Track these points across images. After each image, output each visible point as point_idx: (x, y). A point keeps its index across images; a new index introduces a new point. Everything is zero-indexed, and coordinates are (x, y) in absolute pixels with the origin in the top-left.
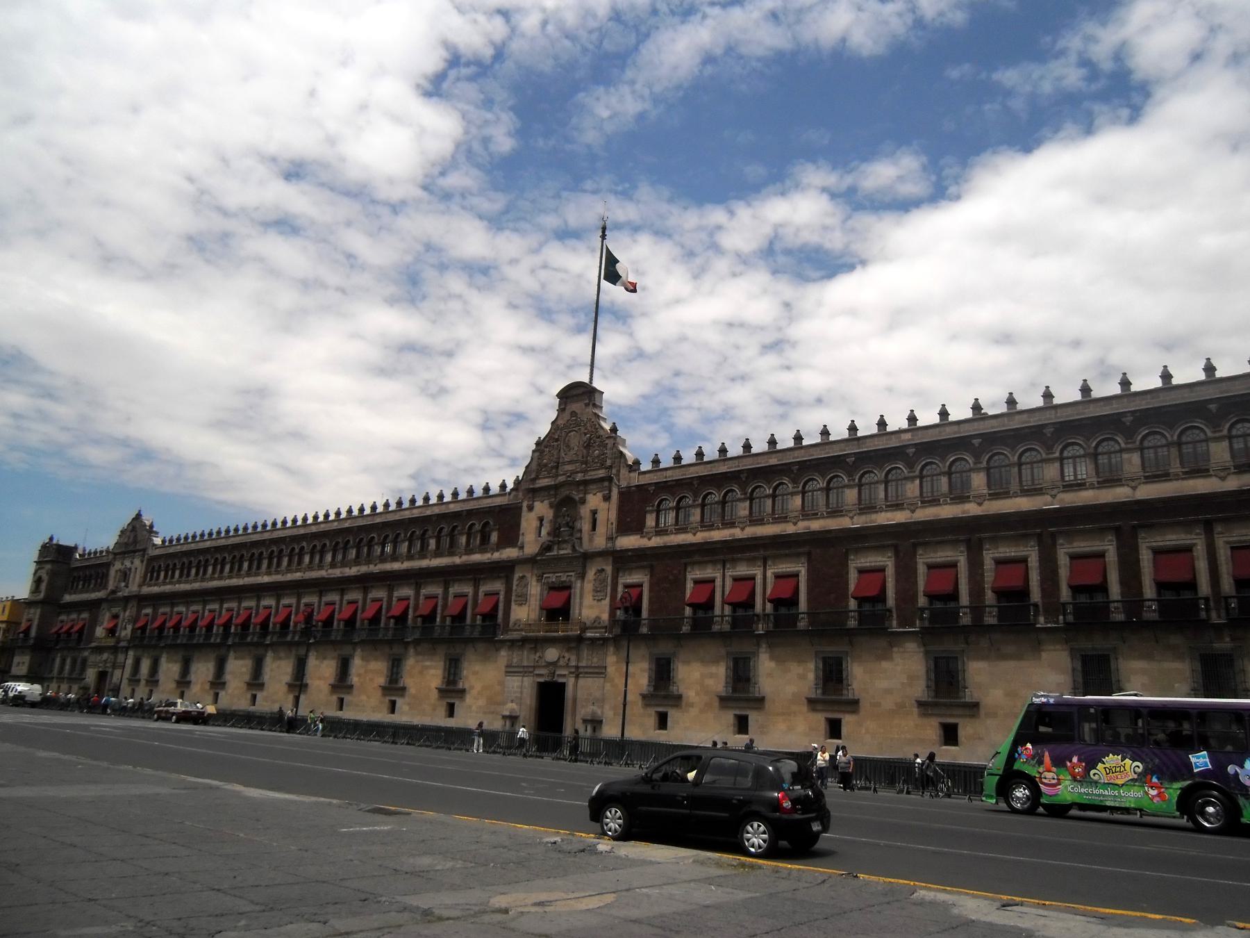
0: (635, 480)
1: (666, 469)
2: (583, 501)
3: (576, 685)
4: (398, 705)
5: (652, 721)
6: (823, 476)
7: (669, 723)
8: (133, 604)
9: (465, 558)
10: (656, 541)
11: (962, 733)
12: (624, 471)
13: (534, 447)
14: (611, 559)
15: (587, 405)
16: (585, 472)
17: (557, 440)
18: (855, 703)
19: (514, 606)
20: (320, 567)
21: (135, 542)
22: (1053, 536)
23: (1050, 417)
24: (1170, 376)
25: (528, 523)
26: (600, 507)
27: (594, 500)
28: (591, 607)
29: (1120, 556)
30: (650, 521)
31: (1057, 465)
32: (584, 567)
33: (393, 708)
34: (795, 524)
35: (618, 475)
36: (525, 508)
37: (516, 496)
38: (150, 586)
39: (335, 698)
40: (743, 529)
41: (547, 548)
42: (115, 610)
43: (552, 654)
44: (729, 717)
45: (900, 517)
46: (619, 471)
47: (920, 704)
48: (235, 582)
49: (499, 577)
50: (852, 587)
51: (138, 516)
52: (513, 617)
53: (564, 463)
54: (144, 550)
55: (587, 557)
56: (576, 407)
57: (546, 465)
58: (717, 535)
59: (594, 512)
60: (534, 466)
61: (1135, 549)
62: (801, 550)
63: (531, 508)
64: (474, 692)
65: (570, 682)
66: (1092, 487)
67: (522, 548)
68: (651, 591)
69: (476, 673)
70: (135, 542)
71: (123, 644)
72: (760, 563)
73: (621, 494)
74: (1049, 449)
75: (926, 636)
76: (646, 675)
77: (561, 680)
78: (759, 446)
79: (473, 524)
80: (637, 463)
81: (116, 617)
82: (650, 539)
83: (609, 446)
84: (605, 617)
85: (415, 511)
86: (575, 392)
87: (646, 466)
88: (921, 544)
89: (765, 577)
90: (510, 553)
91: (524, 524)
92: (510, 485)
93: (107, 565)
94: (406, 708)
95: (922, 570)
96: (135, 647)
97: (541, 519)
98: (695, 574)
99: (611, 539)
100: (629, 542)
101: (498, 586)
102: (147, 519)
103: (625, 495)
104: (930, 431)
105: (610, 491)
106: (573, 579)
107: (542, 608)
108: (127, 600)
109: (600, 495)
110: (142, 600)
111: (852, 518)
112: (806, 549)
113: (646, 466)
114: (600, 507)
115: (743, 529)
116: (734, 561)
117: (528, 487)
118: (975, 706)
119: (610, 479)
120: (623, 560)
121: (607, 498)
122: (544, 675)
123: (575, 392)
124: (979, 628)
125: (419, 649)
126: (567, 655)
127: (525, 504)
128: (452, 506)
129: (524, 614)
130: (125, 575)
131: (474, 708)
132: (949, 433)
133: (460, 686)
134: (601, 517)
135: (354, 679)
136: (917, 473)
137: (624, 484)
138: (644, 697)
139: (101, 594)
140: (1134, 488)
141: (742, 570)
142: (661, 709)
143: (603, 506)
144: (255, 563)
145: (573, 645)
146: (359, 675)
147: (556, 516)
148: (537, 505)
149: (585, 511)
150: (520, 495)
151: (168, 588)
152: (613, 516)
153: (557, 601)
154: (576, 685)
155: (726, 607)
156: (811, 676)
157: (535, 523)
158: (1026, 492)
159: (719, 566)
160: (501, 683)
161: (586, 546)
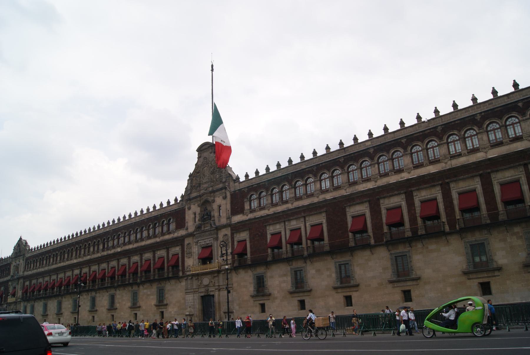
0: (238, 187)
1: (251, 179)
2: (214, 201)
3: (219, 295)
4: (138, 315)
5: (258, 309)
6: (329, 170)
7: (266, 309)
8: (21, 281)
9: (162, 238)
10: (251, 216)
11: (413, 294)
12: (232, 183)
13: (188, 178)
14: (230, 228)
15: (211, 153)
17: (199, 172)
18: (357, 286)
19: (186, 259)
20: (98, 252)
21: (20, 251)
22: (448, 184)
23: (440, 122)
24: (496, 92)
25: (189, 216)
26: (221, 205)
27: (219, 200)
29: (484, 189)
30: (247, 207)
31: (446, 146)
32: (217, 234)
34: (318, 197)
35: (229, 186)
36: (187, 209)
37: (182, 204)
38: (27, 271)
39: (109, 315)
40: (292, 204)
41: (198, 228)
42: (14, 285)
43: (206, 281)
44: (295, 302)
45: (370, 185)
46: (229, 184)
48: (62, 264)
49: (178, 246)
50: (349, 225)
51: (21, 239)
52: (186, 265)
53: (203, 184)
54: (24, 255)
56: (206, 154)
57: (194, 186)
59: (220, 206)
60: (189, 188)
61: (491, 184)
62: (322, 210)
63: (189, 209)
66: (465, 155)
67: (187, 229)
68: (250, 242)
70: (20, 251)
71: (19, 300)
72: (302, 220)
73: (232, 195)
74: (441, 139)
76: (252, 285)
77: (212, 293)
79: (164, 221)
80: (238, 178)
81: (15, 288)
82: (247, 216)
83: (223, 172)
85: (137, 218)
86: (204, 148)
87: (242, 179)
88: (381, 198)
89: (305, 226)
90: (182, 233)
91: (187, 217)
92: (179, 199)
93: (9, 264)
95: (384, 212)
96: (24, 301)
98: (271, 229)
99: (229, 218)
100: (237, 218)
102: (23, 238)
103: (234, 196)
104: (380, 138)
105: (226, 193)
106: (212, 241)
107: (199, 258)
108: (18, 279)
109: (221, 197)
110: (25, 278)
111: (346, 190)
112: (325, 209)
113: (242, 179)
114: (221, 205)
115: (292, 204)
116: (289, 220)
117: (187, 198)
118: (418, 279)
119: (226, 188)
120: (236, 228)
121: (225, 198)
123: (204, 148)
124: (416, 237)
125: (145, 286)
126: (213, 280)
127: (186, 207)
128: (153, 213)
130: (17, 267)
132: (389, 139)
133: (165, 302)
134: (223, 208)
135: (117, 305)
136: (376, 161)
137: (232, 190)
138: (253, 297)
139: (9, 278)
140: (486, 152)
142: (261, 302)
143: (224, 202)
144: (70, 254)
145: (216, 275)
146: (119, 303)
147: (201, 211)
149: (215, 206)
150: (184, 203)
151: (35, 271)
152: (229, 207)
153: (206, 255)
154: (219, 295)
155: (288, 245)
156: (334, 275)
157: (192, 216)
158: (432, 163)
159: (283, 224)
160: (184, 299)
161: (217, 224)
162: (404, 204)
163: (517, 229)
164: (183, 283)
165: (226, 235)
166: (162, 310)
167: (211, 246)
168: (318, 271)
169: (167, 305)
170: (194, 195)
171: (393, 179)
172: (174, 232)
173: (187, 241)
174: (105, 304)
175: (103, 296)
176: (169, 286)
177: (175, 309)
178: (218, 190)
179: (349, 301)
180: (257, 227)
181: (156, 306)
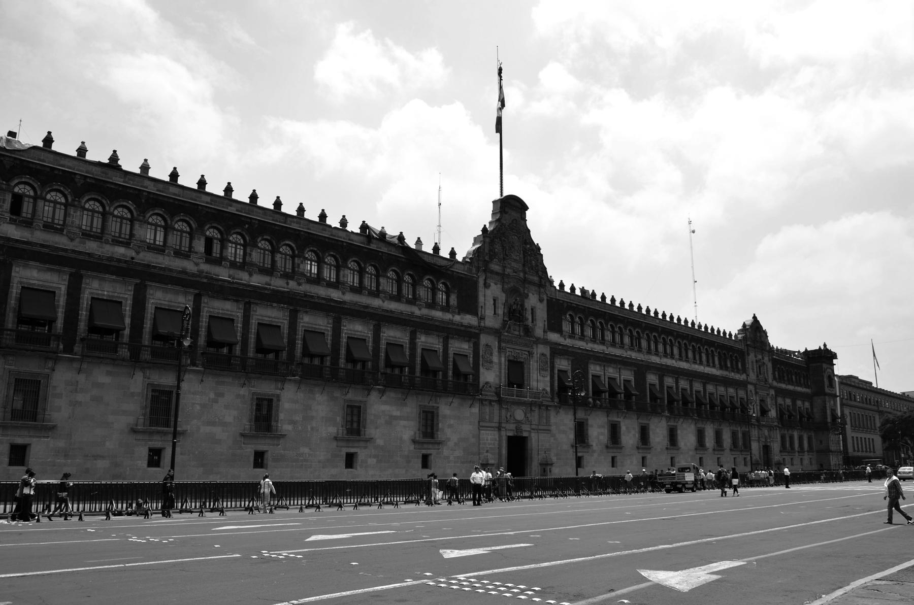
2: (527, 296)
16: (525, 273)
19: (482, 370)
28: (539, 381)
33: (350, 460)
47: (638, 448)
49: (469, 341)
55: (538, 341)
58: (598, 348)
63: (486, 286)
64: (451, 444)
65: (534, 436)
67: (482, 318)
69: (450, 426)
75: (668, 419)
78: (445, 253)
84: (548, 389)
94: (372, 461)
99: (545, 332)
100: (554, 337)
101: (465, 347)
121: (541, 300)
122: (510, 430)
129: (491, 376)
131: (452, 458)
150: (474, 270)
164: (475, 410)
165: (543, 354)
166: (429, 452)
167: (522, 363)
168: (627, 428)
169: (439, 443)
172: (453, 313)
173: (484, 339)
174: (229, 419)
175: (221, 395)
177: (458, 453)
178: (534, 284)
180: (581, 360)
181: (414, 441)
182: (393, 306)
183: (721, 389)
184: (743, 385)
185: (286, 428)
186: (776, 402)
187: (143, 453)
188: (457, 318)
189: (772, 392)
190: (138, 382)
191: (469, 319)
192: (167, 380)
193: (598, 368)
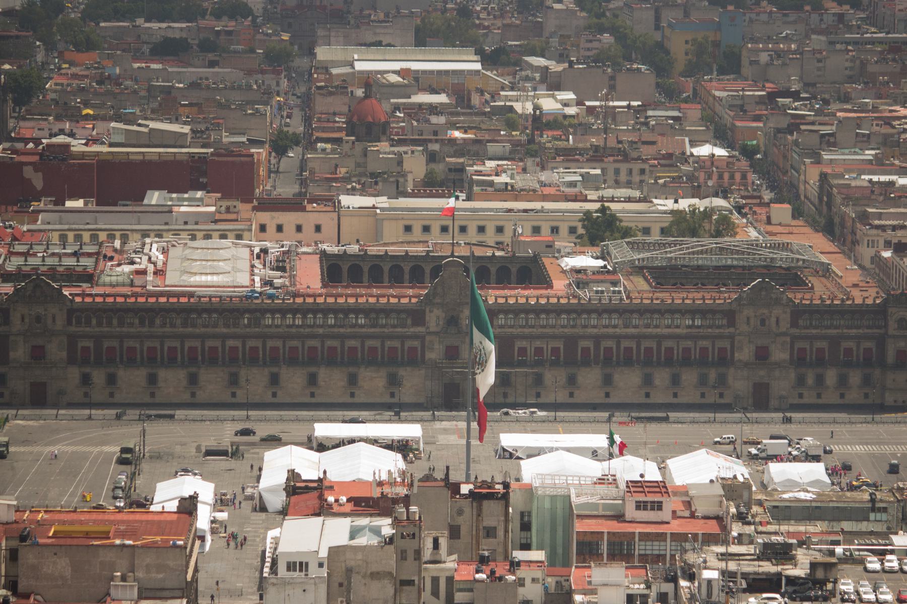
19: (426, 353)
56: (453, 269)
63: (431, 311)
67: (428, 328)
89: (547, 347)
91: (427, 318)
95: (602, 348)
97: (438, 318)
101: (416, 343)
124: (618, 364)
141: (538, 343)
148: (435, 311)
162: (614, 347)
163: (667, 370)
164: (423, 372)
170: (438, 300)
171: (611, 331)
173: (428, 338)
176: (403, 372)
179: (571, 395)
182: (373, 330)
183: (689, 343)
184: (732, 337)
185: (322, 383)
186: (792, 347)
187: (270, 393)
188: (412, 330)
189: (788, 339)
190: (266, 371)
191: (420, 329)
192: (275, 370)
193: (524, 343)
